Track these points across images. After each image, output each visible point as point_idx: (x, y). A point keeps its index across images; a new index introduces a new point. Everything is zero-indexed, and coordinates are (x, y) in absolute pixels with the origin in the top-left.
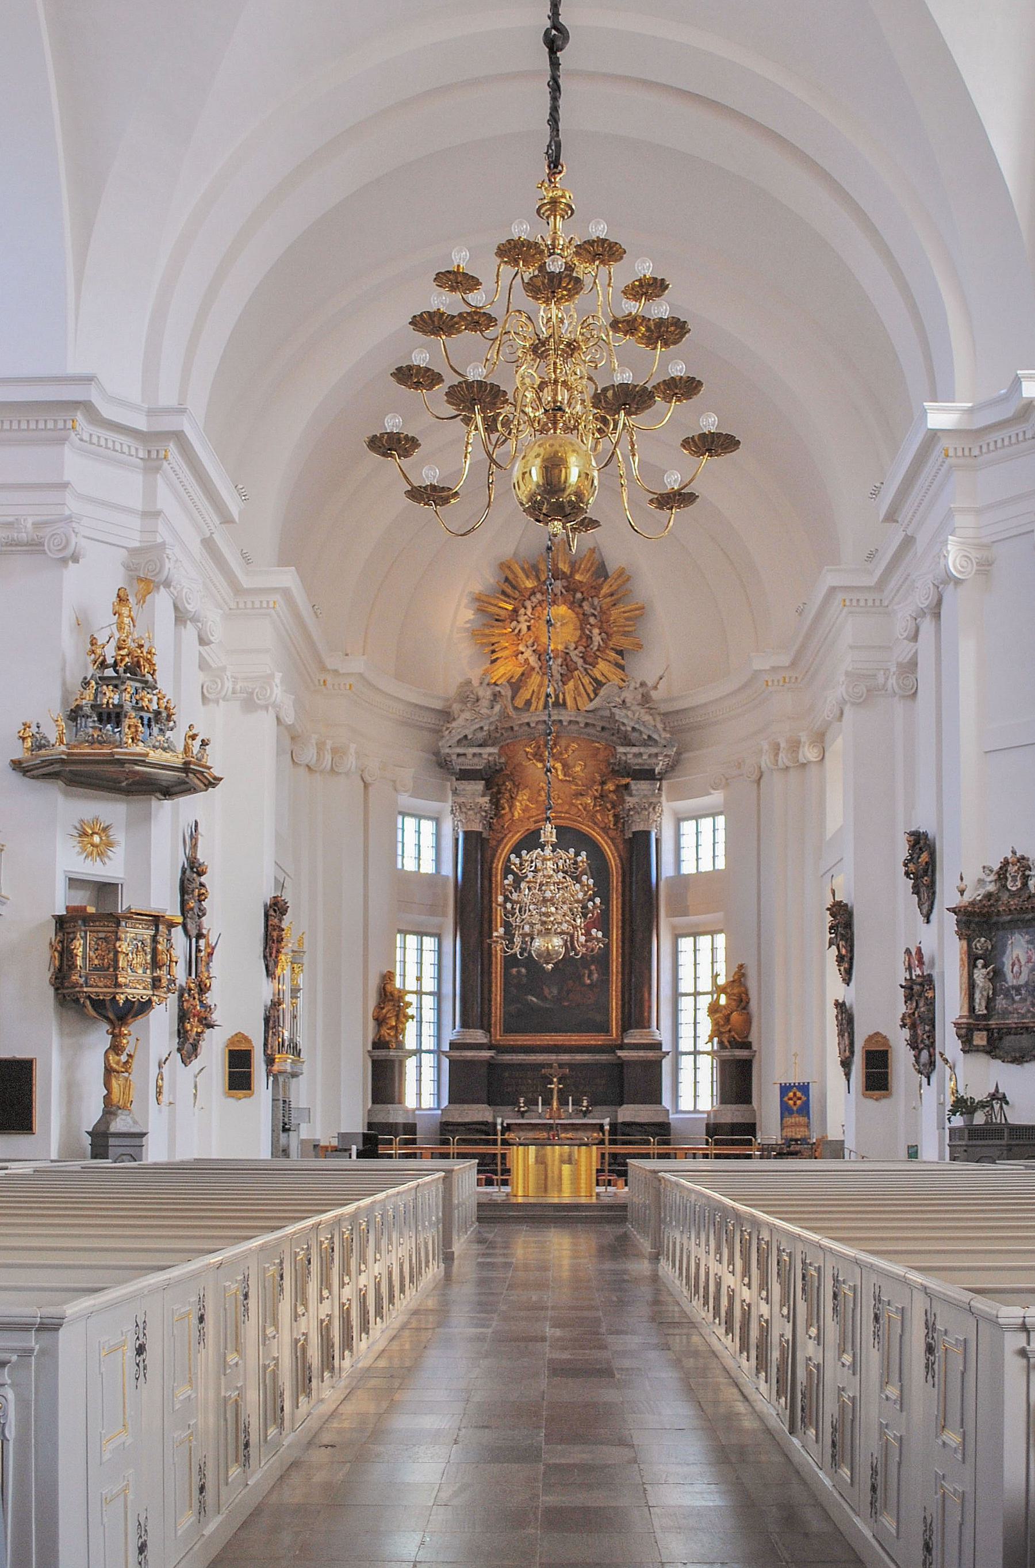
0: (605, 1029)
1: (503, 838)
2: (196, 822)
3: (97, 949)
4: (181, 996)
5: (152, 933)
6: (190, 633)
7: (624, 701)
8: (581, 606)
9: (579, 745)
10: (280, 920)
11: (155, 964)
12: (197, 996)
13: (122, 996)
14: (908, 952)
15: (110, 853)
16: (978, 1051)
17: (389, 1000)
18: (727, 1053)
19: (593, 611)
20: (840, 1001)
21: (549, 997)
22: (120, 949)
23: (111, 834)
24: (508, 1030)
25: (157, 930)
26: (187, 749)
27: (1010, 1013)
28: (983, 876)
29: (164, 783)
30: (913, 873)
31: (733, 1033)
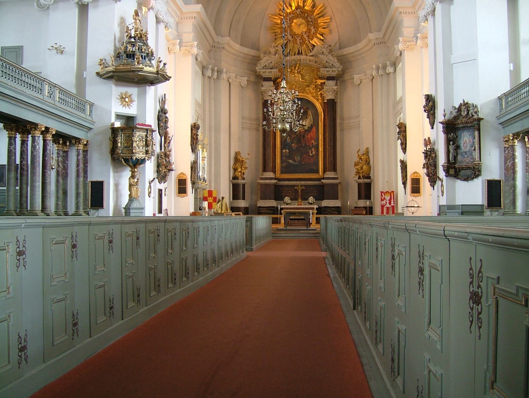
0: (317, 172)
2: (165, 95)
4: (158, 158)
5: (146, 134)
6: (162, 26)
7: (323, 52)
8: (307, 18)
9: (307, 68)
10: (197, 132)
11: (147, 145)
12: (164, 158)
13: (135, 157)
14: (425, 140)
16: (451, 176)
17: (238, 162)
18: (361, 181)
19: (311, 20)
20: (402, 160)
21: (297, 161)
22: (133, 140)
24: (282, 172)
26: (158, 67)
27: (463, 162)
28: (452, 110)
29: (151, 79)
30: (427, 111)
31: (364, 173)
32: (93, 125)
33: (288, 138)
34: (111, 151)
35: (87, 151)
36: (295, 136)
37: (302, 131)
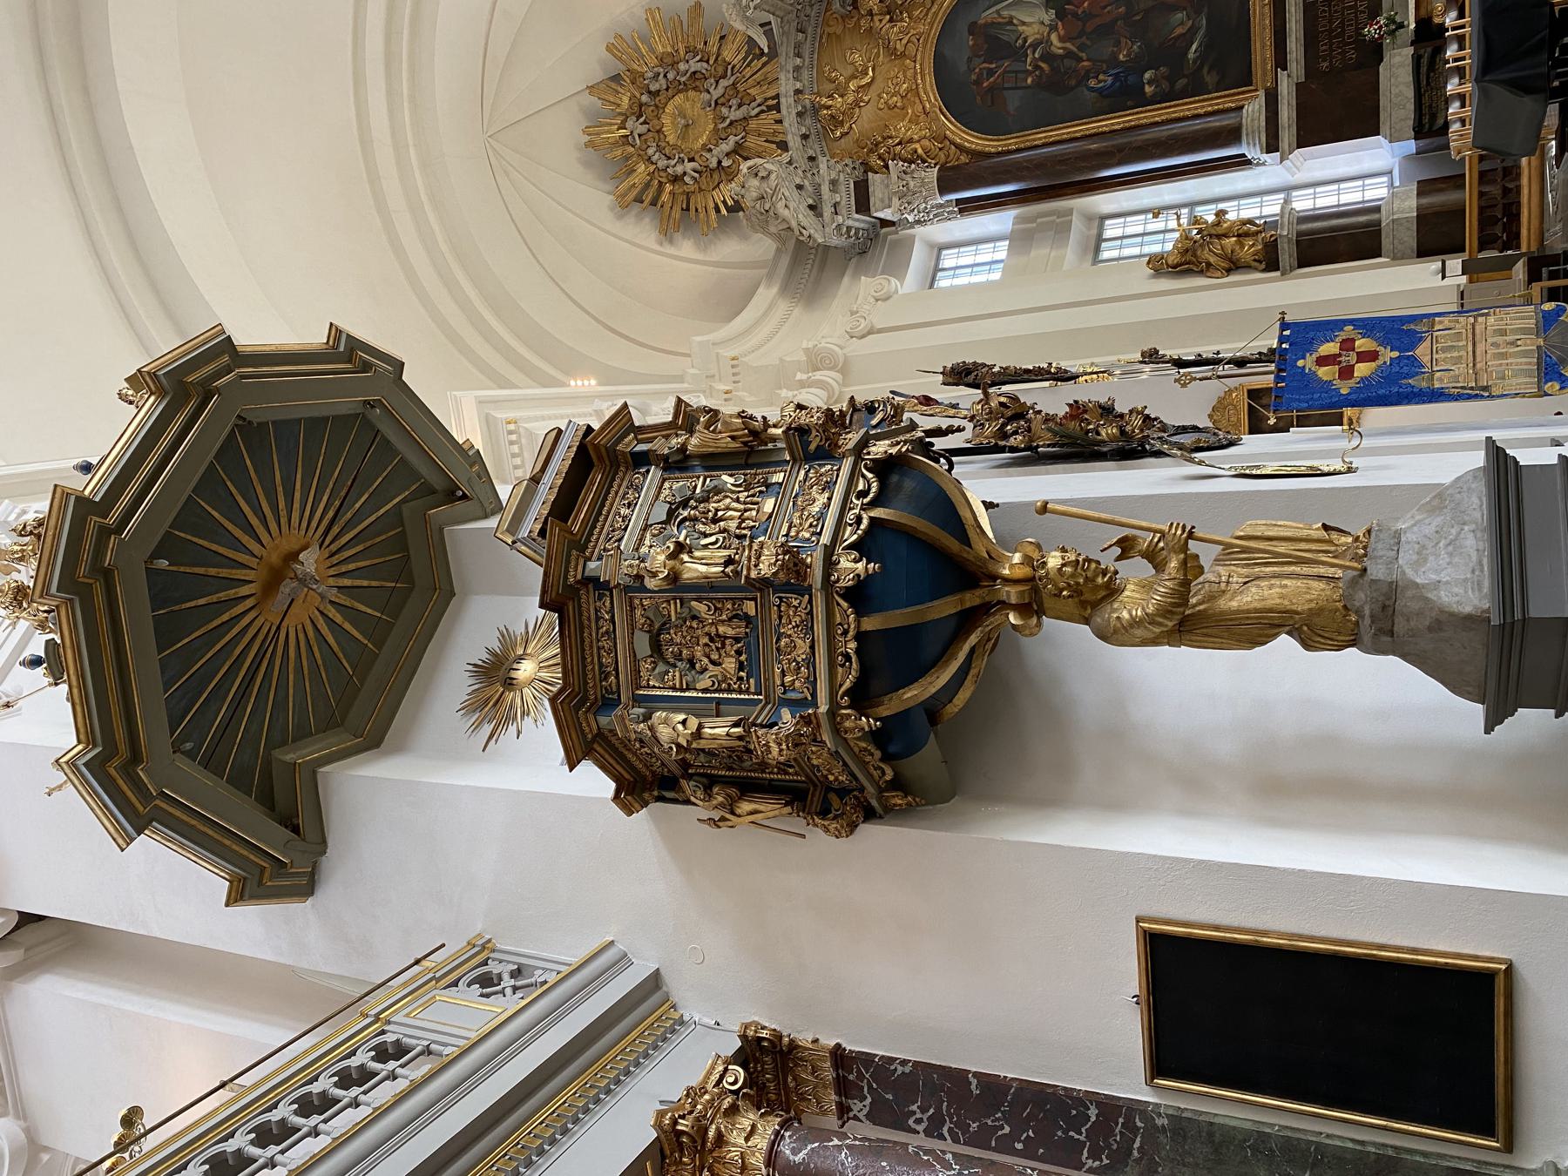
1: (954, 144)
9: (827, 64)
33: (1092, 83)
34: (824, 812)
36: (1083, 55)
37: (1062, 33)
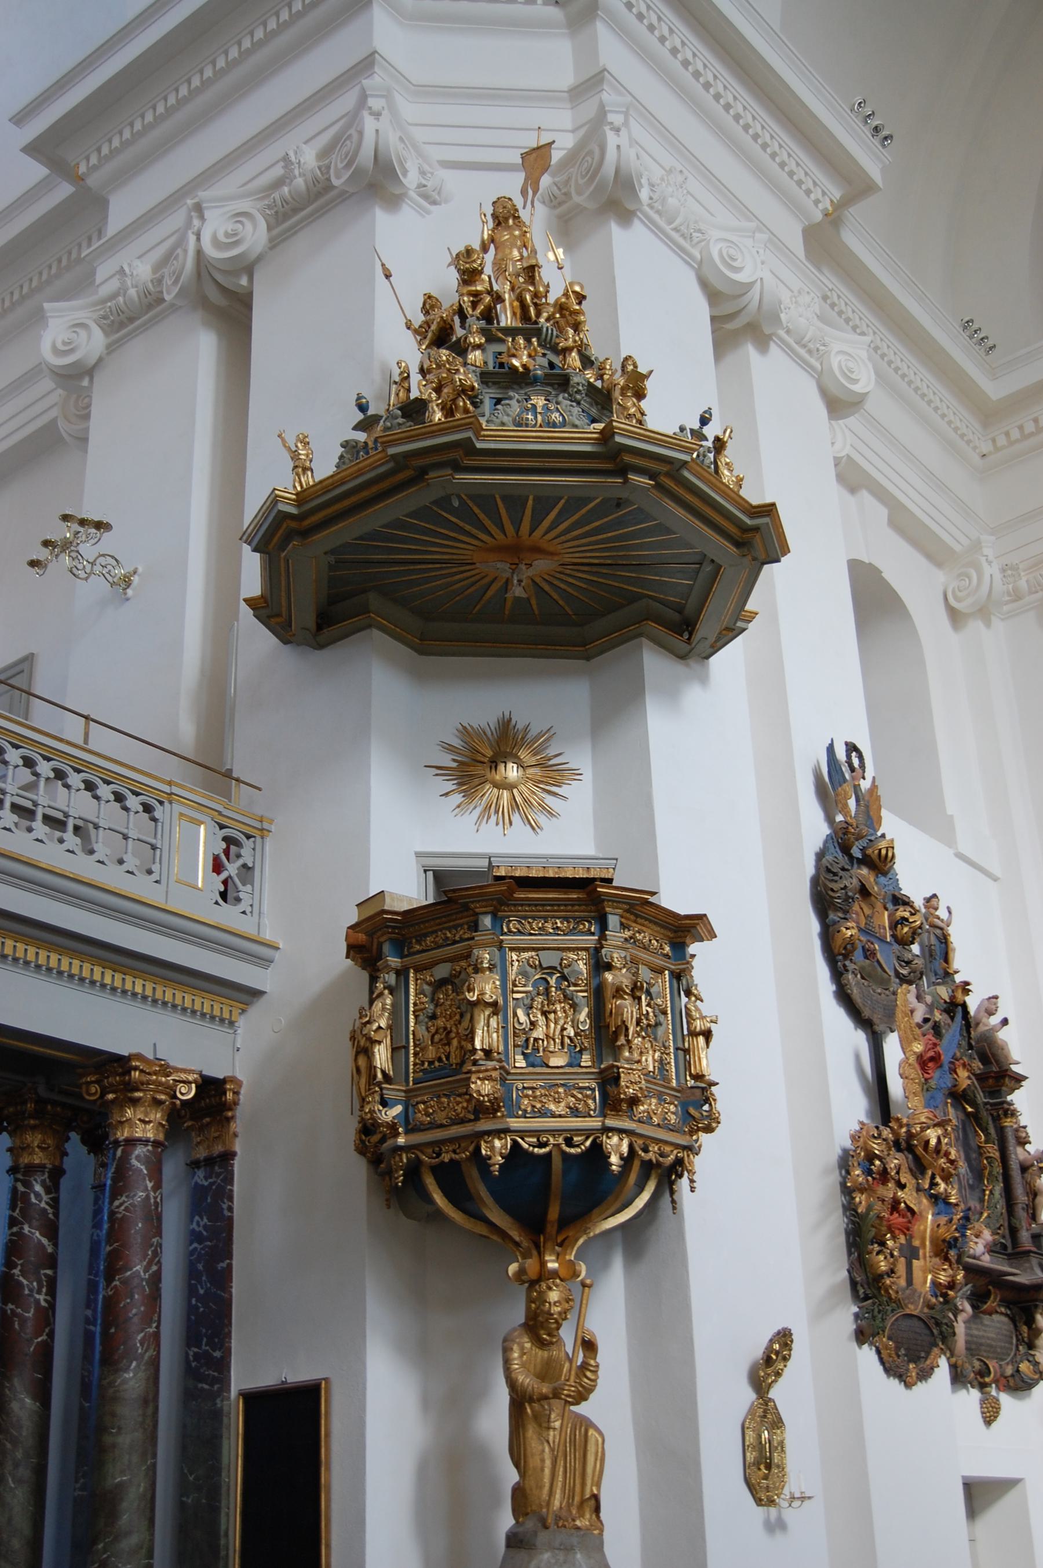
3: (433, 1017)
13: (497, 1143)
15: (549, 800)
23: (551, 752)
25: (604, 926)
32: (265, 962)
35: (228, 1156)
